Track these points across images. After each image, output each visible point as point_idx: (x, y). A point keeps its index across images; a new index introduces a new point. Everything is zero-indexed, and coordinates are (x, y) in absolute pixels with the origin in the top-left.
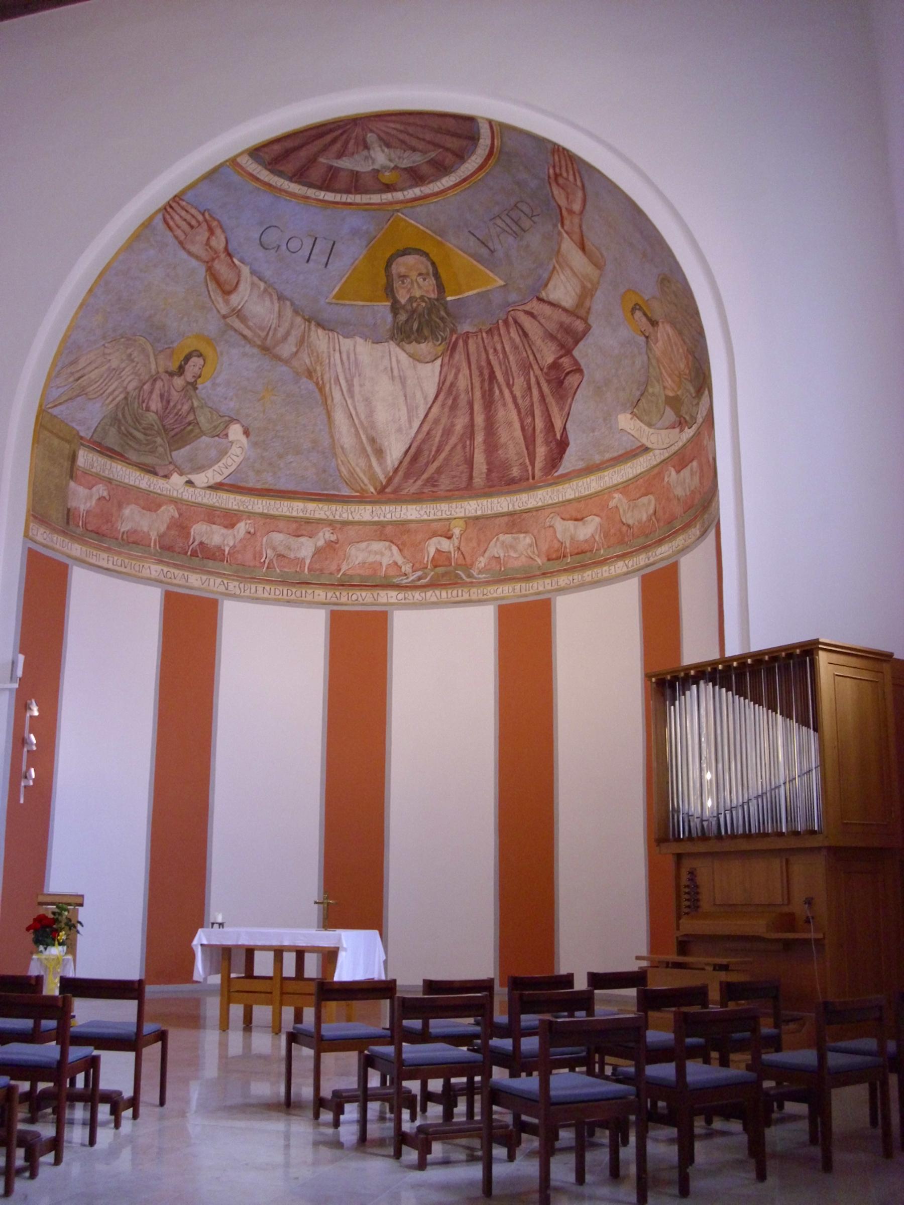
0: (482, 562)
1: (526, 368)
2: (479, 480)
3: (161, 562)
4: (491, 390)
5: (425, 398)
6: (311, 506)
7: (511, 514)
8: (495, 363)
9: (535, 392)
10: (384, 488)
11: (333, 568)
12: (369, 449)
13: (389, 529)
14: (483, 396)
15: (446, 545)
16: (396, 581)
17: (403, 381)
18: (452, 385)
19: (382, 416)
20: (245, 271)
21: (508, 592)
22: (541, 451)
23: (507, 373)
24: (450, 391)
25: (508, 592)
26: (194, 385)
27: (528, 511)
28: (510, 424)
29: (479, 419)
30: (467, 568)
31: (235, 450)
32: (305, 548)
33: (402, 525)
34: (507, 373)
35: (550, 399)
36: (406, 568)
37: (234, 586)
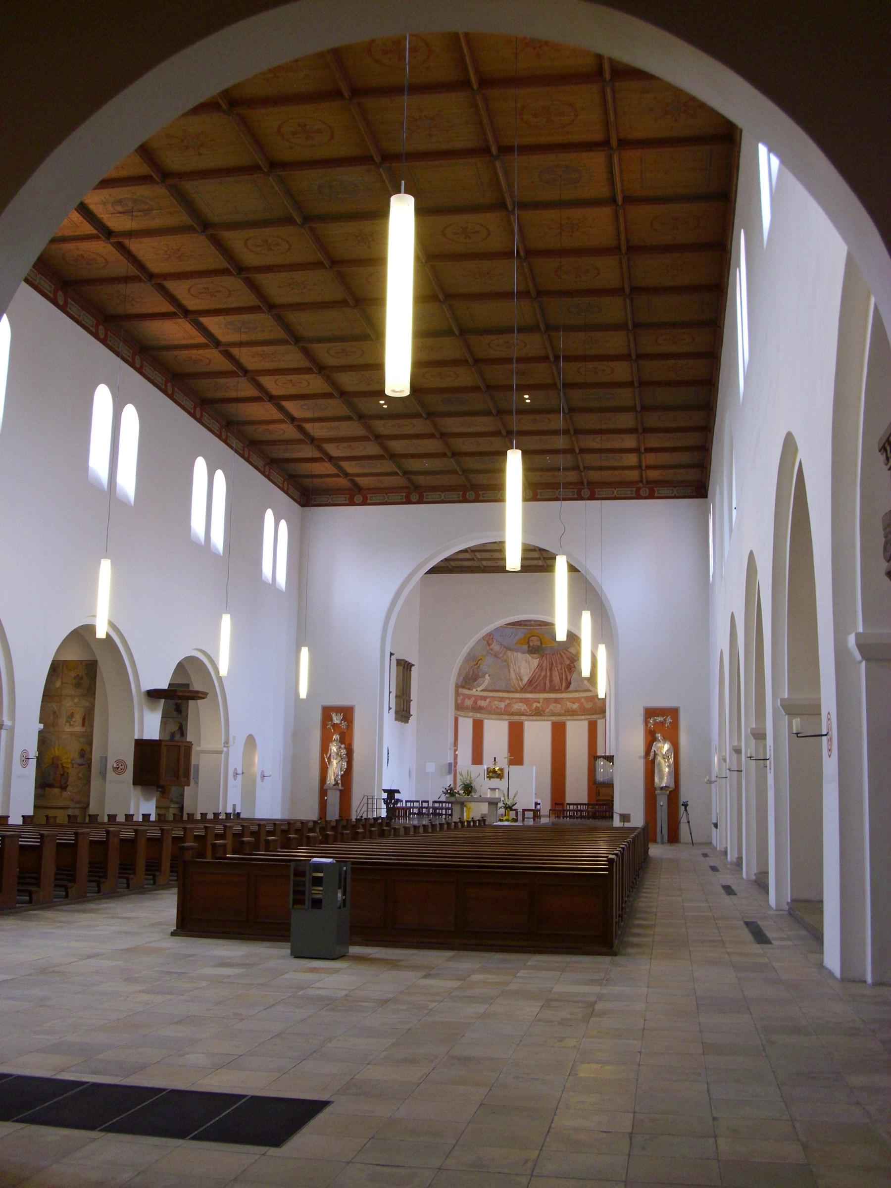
0: (548, 710)
1: (561, 664)
2: (547, 689)
3: (472, 712)
4: (552, 668)
5: (534, 667)
6: (504, 694)
7: (556, 698)
8: (554, 663)
9: (563, 670)
10: (522, 689)
11: (510, 710)
12: (519, 679)
13: (523, 700)
14: (550, 668)
15: (538, 705)
16: (525, 714)
17: (529, 662)
18: (542, 665)
19: (523, 671)
20: (495, 641)
21: (553, 718)
22: (564, 684)
23: (556, 664)
24: (540, 667)
25: (554, 718)
26: (479, 667)
27: (560, 698)
28: (556, 676)
29: (548, 674)
30: (544, 711)
31: (487, 681)
32: (502, 705)
33: (526, 699)
34: (556, 664)
35: (567, 672)
36: (528, 710)
37: (486, 716)
